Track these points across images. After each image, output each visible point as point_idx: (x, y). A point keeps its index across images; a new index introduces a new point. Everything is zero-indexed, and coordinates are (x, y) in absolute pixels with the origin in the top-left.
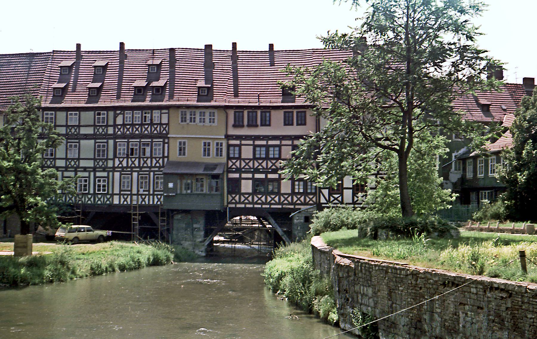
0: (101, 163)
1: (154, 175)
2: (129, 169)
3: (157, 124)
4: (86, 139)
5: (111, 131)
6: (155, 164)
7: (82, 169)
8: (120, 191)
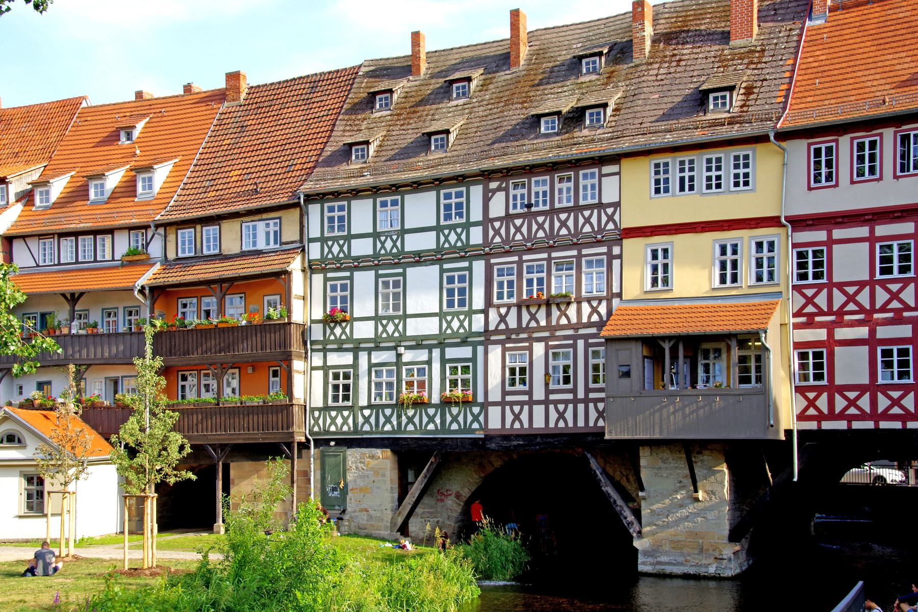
0: (455, 324)
1: (587, 346)
3: (590, 207)
4: (418, 263)
5: (476, 236)
6: (590, 316)
7: (413, 343)
8: (505, 393)
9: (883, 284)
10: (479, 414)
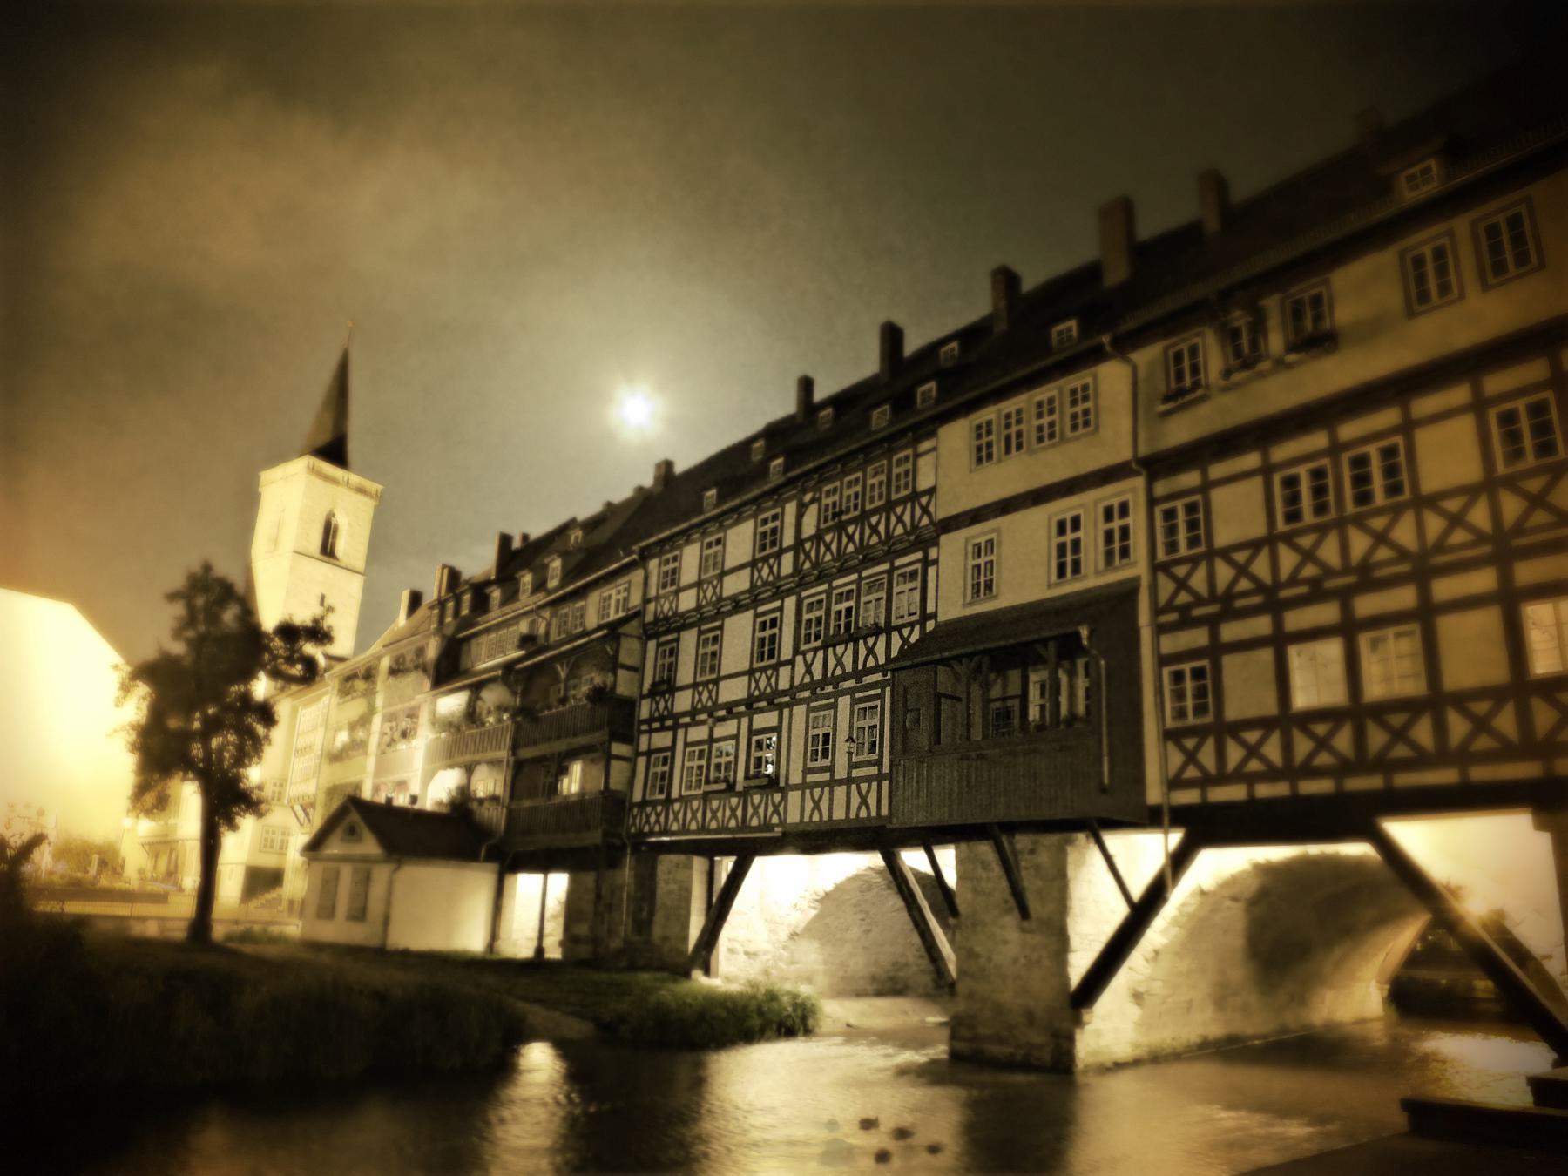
2: (829, 689)
3: (903, 501)
8: (807, 771)
9: (1288, 539)
10: (780, 803)
